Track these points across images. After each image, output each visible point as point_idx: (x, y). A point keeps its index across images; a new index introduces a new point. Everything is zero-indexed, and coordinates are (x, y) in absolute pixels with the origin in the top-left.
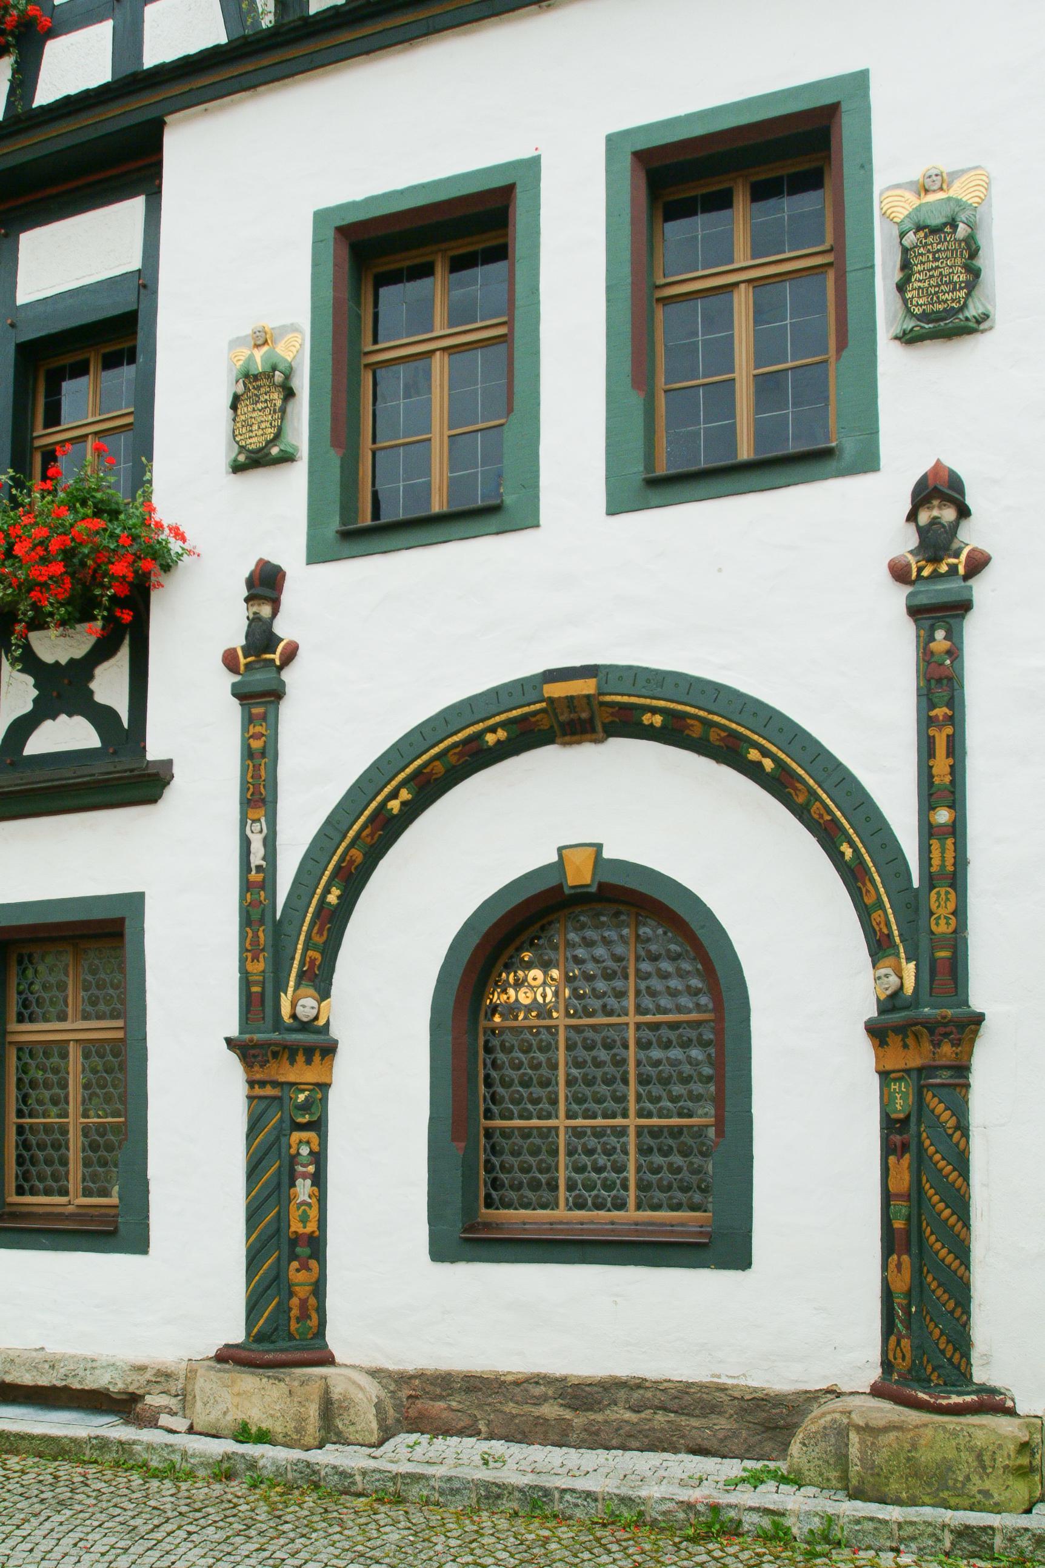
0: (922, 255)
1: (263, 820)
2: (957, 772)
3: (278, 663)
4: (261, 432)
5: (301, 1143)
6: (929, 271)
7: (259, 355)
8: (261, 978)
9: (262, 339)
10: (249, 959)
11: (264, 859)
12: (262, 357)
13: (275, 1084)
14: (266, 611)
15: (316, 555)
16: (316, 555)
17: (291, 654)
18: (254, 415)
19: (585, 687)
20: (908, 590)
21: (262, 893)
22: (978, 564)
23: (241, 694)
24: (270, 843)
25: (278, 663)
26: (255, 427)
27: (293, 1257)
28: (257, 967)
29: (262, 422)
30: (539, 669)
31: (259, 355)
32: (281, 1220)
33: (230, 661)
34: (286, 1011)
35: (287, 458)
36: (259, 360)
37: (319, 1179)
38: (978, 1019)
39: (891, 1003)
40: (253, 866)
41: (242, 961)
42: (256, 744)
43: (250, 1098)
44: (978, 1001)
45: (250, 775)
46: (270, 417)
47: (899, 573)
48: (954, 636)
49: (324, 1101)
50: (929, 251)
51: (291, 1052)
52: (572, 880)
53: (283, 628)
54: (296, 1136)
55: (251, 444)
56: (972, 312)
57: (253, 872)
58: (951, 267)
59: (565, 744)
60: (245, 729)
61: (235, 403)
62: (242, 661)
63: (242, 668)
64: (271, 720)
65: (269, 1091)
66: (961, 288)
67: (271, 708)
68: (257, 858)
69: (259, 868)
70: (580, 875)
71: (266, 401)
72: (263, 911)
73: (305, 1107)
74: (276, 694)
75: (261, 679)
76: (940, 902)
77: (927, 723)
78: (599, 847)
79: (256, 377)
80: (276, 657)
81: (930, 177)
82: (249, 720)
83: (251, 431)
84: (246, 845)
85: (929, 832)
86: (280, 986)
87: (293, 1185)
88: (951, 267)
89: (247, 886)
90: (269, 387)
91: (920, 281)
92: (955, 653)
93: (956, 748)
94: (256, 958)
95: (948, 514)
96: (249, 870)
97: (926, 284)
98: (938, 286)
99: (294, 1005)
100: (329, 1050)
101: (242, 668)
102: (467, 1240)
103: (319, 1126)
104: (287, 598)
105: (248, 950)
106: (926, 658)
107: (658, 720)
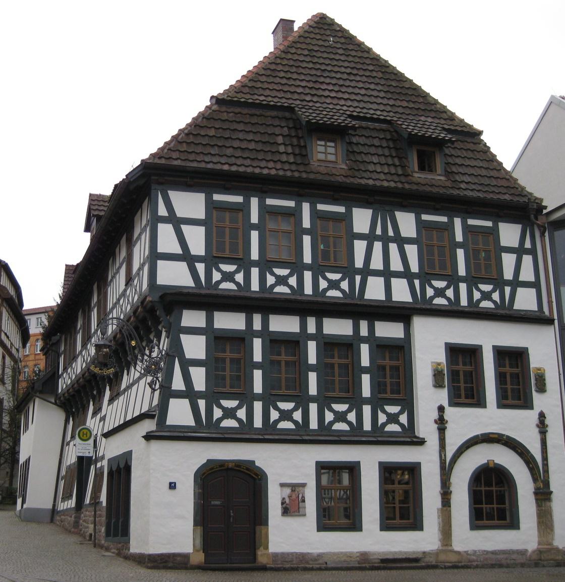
9: (439, 364)
15: (450, 405)
16: (450, 405)
17: (447, 422)
19: (496, 436)
24: (445, 455)
33: (436, 422)
35: (445, 387)
38: (552, 492)
44: (552, 489)
53: (446, 418)
64: (444, 433)
70: (491, 465)
75: (442, 426)
78: (494, 461)
82: (440, 433)
94: (444, 476)
95: (543, 419)
104: (446, 411)
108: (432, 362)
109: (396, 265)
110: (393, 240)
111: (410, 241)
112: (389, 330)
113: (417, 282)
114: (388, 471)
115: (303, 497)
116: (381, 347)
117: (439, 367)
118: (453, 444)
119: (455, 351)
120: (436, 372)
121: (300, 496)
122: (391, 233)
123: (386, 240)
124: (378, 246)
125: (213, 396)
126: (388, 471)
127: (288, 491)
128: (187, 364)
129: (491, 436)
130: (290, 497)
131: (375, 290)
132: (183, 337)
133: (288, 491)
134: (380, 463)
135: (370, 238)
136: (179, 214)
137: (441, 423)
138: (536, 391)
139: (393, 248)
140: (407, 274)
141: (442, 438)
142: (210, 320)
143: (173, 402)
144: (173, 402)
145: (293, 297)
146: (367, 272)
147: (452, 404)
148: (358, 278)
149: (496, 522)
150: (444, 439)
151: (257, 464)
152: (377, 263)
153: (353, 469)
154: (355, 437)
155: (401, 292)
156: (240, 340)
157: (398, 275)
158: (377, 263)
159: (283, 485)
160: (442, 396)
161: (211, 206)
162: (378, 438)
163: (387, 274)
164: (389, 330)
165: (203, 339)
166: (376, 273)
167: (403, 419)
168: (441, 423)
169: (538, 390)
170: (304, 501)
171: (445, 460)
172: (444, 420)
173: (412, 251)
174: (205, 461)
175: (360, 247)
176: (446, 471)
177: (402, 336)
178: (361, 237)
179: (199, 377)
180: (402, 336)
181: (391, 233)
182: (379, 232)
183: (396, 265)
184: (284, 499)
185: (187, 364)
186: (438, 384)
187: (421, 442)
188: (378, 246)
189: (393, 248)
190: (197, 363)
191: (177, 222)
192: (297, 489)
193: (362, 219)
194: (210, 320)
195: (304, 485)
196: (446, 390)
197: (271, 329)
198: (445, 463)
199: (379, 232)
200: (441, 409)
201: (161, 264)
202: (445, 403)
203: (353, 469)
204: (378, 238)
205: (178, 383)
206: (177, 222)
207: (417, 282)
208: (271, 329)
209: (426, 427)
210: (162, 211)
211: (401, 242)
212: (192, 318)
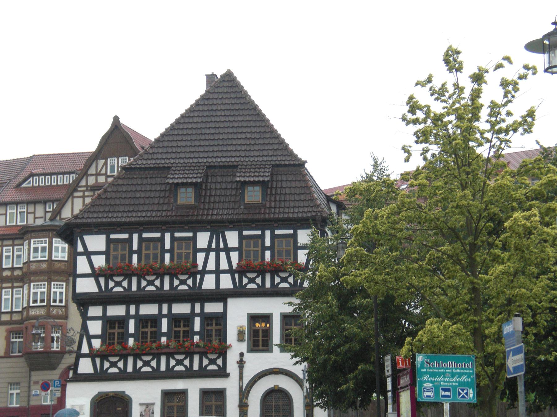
9: (241, 327)
17: (245, 362)
24: (242, 383)
30: (272, 367)
31: (241, 329)
33: (238, 362)
35: (245, 341)
51: (245, 406)
52: (275, 389)
53: (244, 359)
61: (238, 334)
70: (276, 388)
100: (248, 406)
104: (244, 356)
105: (240, 395)
108: (238, 326)
109: (224, 265)
110: (222, 250)
111: (234, 249)
112: (213, 308)
113: (237, 276)
114: (205, 394)
115: (153, 411)
116: (207, 319)
117: (241, 329)
118: (248, 376)
119: (253, 318)
121: (151, 411)
122: (222, 245)
123: (218, 250)
124: (213, 255)
125: (104, 356)
126: (205, 394)
127: (144, 407)
128: (90, 338)
129: (275, 370)
130: (145, 411)
131: (209, 283)
132: (89, 323)
133: (144, 407)
134: (200, 389)
135: (208, 251)
136: (90, 249)
137: (241, 363)
139: (223, 255)
140: (231, 271)
142: (105, 311)
143: (82, 360)
144: (82, 360)
145: (157, 292)
146: (204, 272)
147: (250, 350)
148: (198, 277)
151: (127, 393)
152: (211, 266)
153: (183, 393)
154: (189, 374)
155: (226, 282)
156: (122, 322)
157: (224, 272)
158: (211, 266)
159: (141, 404)
160: (243, 347)
161: (109, 242)
162: (203, 374)
163: (218, 272)
164: (213, 308)
165: (99, 323)
166: (211, 272)
167: (220, 362)
168: (241, 363)
170: (153, 413)
171: (242, 386)
172: (243, 361)
173: (235, 256)
174: (97, 393)
175: (201, 257)
176: (244, 394)
178: (202, 250)
179: (97, 344)
181: (222, 245)
182: (214, 246)
183: (224, 265)
184: (141, 412)
185: (90, 338)
186: (240, 339)
187: (227, 375)
188: (213, 255)
189: (223, 255)
190: (96, 337)
191: (88, 254)
192: (149, 407)
193: (203, 240)
194: (105, 311)
195: (153, 404)
197: (140, 313)
199: (214, 246)
200: (242, 355)
201: (79, 280)
202: (245, 350)
203: (183, 393)
204: (213, 250)
205: (85, 349)
206: (88, 254)
207: (237, 276)
208: (140, 313)
209: (232, 367)
210: (80, 249)
211: (227, 250)
212: (95, 311)
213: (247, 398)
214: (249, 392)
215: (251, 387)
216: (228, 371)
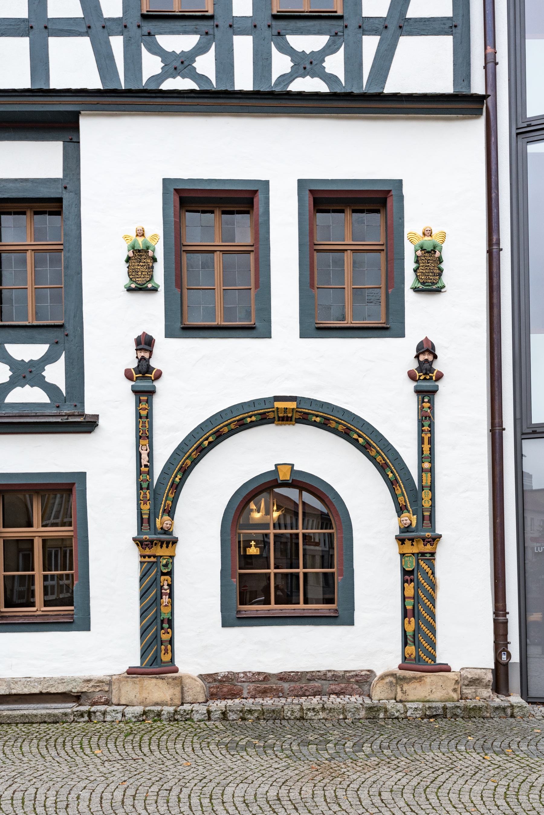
0: (423, 260)
1: (147, 445)
2: (432, 450)
3: (153, 379)
4: (143, 276)
5: (164, 581)
6: (426, 266)
7: (140, 240)
8: (148, 512)
10: (142, 504)
11: (148, 462)
12: (142, 242)
13: (155, 556)
14: (147, 355)
15: (169, 334)
16: (169, 334)
18: (139, 267)
19: (292, 405)
20: (415, 384)
21: (148, 476)
22: (440, 376)
23: (137, 392)
24: (150, 455)
25: (153, 379)
26: (140, 273)
27: (162, 628)
28: (146, 508)
29: (143, 271)
30: (272, 395)
32: (158, 612)
33: (128, 375)
34: (158, 525)
35: (155, 290)
36: (140, 243)
37: (171, 595)
39: (406, 529)
40: (143, 464)
41: (139, 505)
42: (144, 413)
43: (142, 563)
45: (141, 425)
46: (147, 270)
47: (412, 376)
48: (431, 402)
49: (172, 563)
50: (426, 259)
53: (154, 363)
54: (163, 578)
55: (138, 281)
56: (439, 285)
57: (143, 467)
58: (433, 267)
59: (277, 425)
60: (137, 406)
61: (128, 260)
62: (135, 376)
63: (135, 379)
65: (152, 559)
66: (437, 276)
67: (150, 397)
68: (144, 461)
69: (146, 466)
71: (144, 262)
72: (149, 484)
73: (166, 566)
74: (151, 392)
75: (144, 385)
76: (426, 495)
77: (421, 431)
79: (139, 251)
80: (152, 376)
81: (427, 231)
82: (138, 402)
83: (138, 275)
84: (139, 456)
85: (421, 470)
86: (156, 516)
87: (162, 598)
88: (433, 267)
89: (139, 473)
90: (146, 256)
91: (422, 270)
92: (432, 408)
93: (431, 441)
94: (145, 503)
95: (430, 358)
96: (141, 466)
97: (425, 271)
98: (429, 273)
99: (162, 523)
101: (135, 379)
102: (238, 618)
103: (170, 574)
104: (156, 350)
106: (421, 409)
107: (318, 420)
120: (131, 254)
129: (278, 405)
138: (416, 290)
141: (144, 413)
149: (274, 608)
150: (149, 416)
169: (419, 285)
177: (57, 172)
180: (57, 172)
196: (159, 298)
198: (150, 473)
213: (170, 512)
214: (177, 488)
215: (186, 472)
216: (89, 410)
